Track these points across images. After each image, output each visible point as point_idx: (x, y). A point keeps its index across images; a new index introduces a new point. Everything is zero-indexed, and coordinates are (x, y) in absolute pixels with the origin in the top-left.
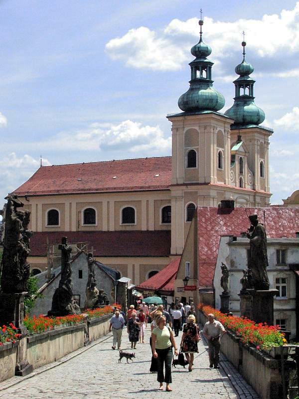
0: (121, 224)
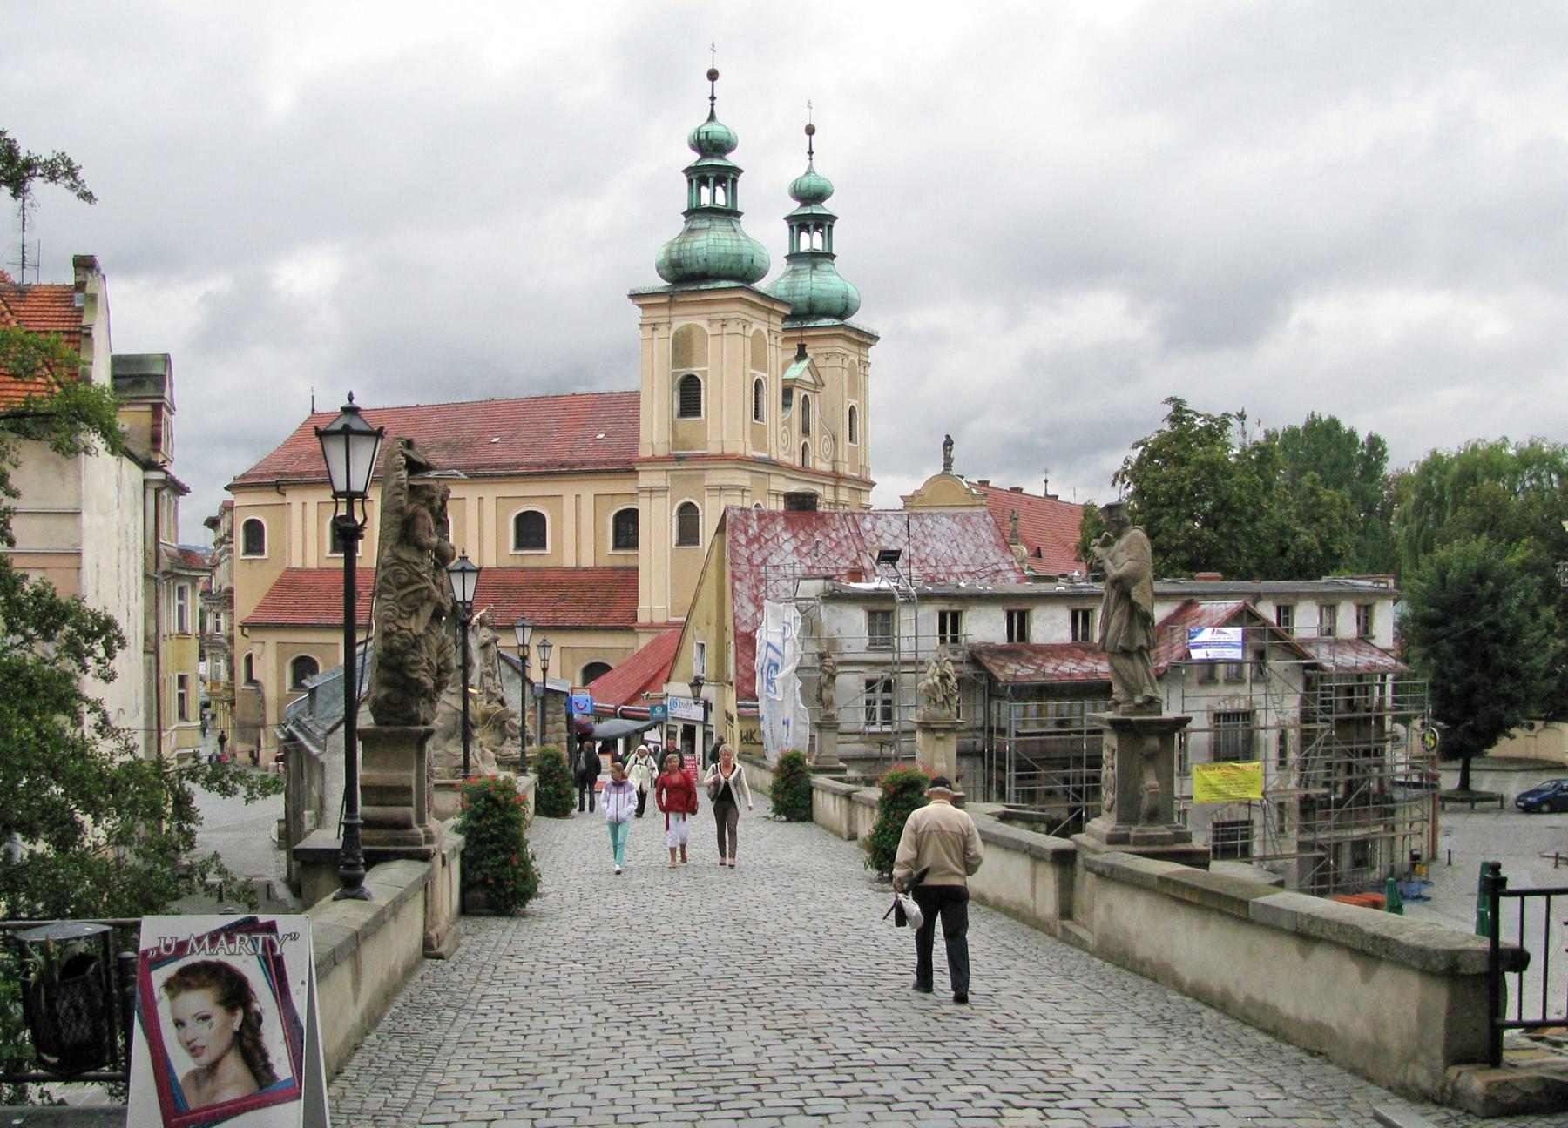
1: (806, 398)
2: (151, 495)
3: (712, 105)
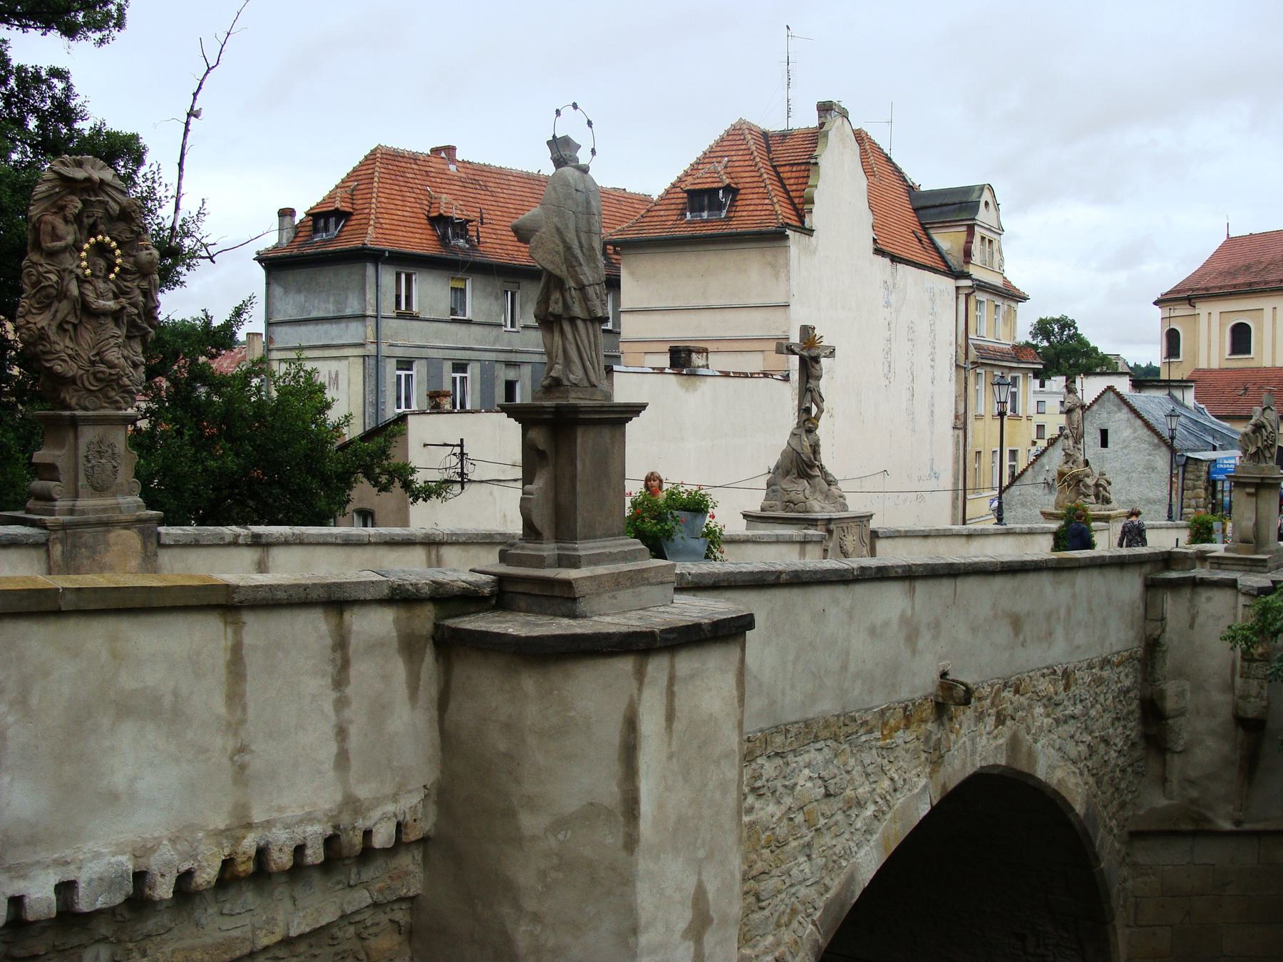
2: (962, 298)
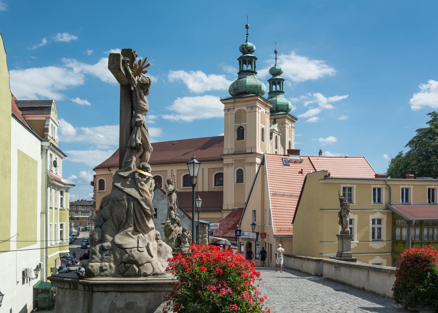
0: (182, 188)
1: (276, 136)
3: (247, 37)
